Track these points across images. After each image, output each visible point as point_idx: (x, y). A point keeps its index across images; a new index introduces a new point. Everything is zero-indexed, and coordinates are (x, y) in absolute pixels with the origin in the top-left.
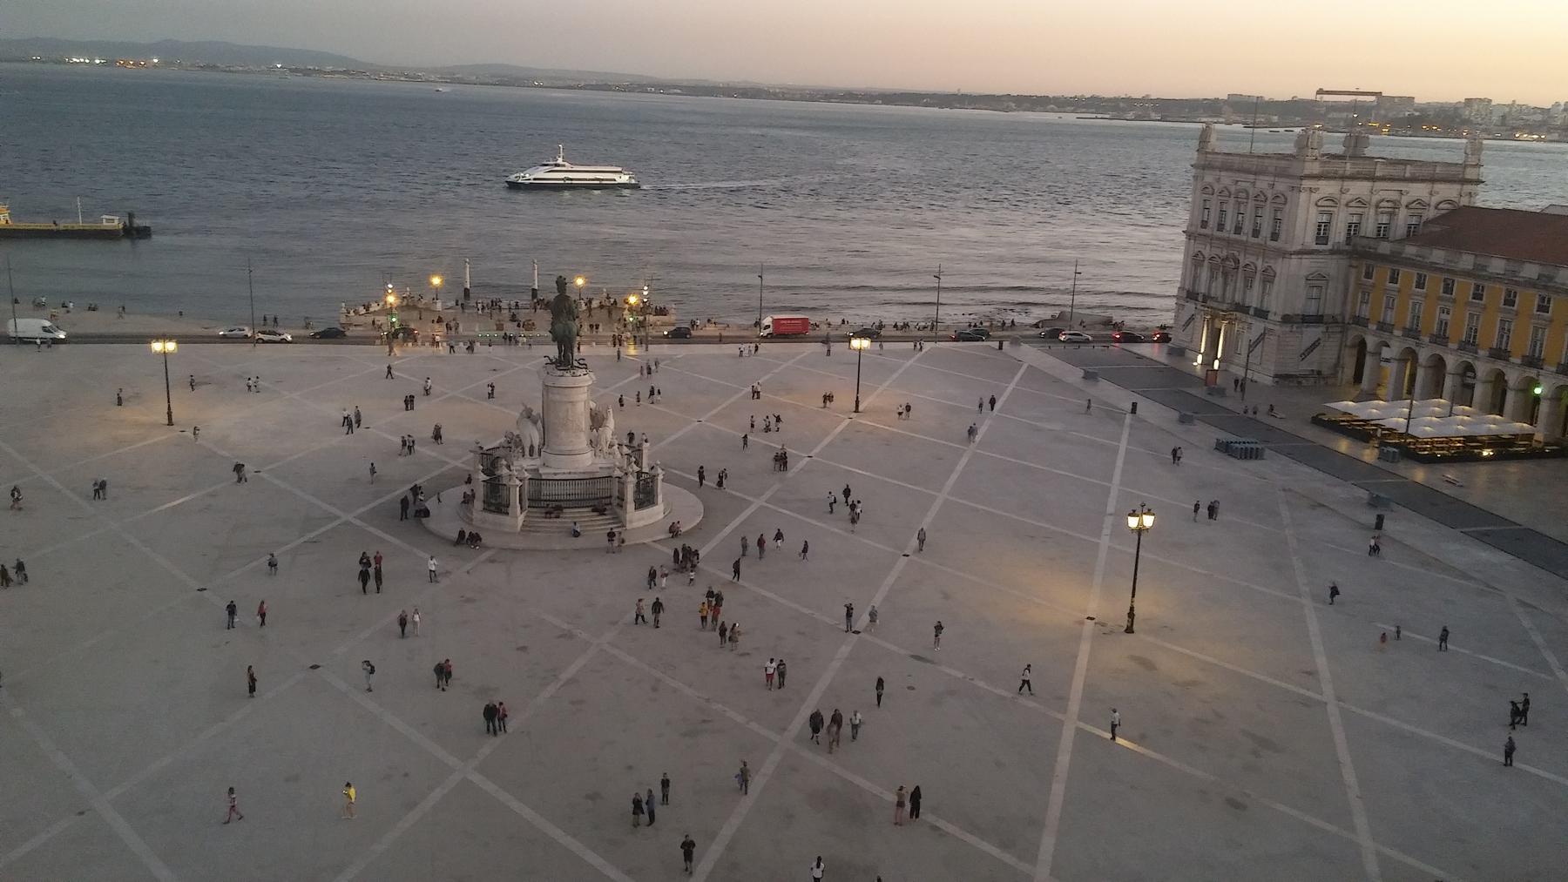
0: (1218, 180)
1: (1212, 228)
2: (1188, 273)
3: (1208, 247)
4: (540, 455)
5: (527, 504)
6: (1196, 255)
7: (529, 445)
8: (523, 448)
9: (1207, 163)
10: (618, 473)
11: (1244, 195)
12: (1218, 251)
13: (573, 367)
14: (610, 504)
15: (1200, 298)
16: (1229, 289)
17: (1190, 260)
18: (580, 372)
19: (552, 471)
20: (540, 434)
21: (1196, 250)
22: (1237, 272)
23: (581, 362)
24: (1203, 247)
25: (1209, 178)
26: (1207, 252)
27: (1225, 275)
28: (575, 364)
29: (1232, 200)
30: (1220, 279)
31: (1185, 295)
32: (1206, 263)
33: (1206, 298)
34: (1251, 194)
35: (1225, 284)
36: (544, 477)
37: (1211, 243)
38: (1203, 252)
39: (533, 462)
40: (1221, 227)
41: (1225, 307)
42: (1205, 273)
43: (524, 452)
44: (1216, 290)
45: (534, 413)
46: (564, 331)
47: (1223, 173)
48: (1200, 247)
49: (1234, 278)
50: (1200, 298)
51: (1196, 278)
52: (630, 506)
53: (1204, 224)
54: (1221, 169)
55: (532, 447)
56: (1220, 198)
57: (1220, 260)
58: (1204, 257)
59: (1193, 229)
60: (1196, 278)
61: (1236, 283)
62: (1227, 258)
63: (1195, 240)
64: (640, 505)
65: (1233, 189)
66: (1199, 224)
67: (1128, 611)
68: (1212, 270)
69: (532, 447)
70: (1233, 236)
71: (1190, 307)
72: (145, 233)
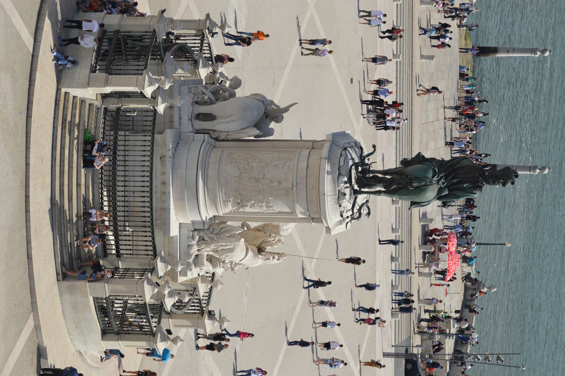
4: (198, 132)
5: (113, 106)
7: (215, 113)
8: (212, 103)
10: (161, 269)
13: (356, 192)
18: (347, 204)
23: (364, 211)
28: (361, 199)
36: (157, 137)
39: (185, 119)
43: (205, 103)
45: (273, 125)
46: (418, 179)
55: (209, 117)
69: (209, 117)
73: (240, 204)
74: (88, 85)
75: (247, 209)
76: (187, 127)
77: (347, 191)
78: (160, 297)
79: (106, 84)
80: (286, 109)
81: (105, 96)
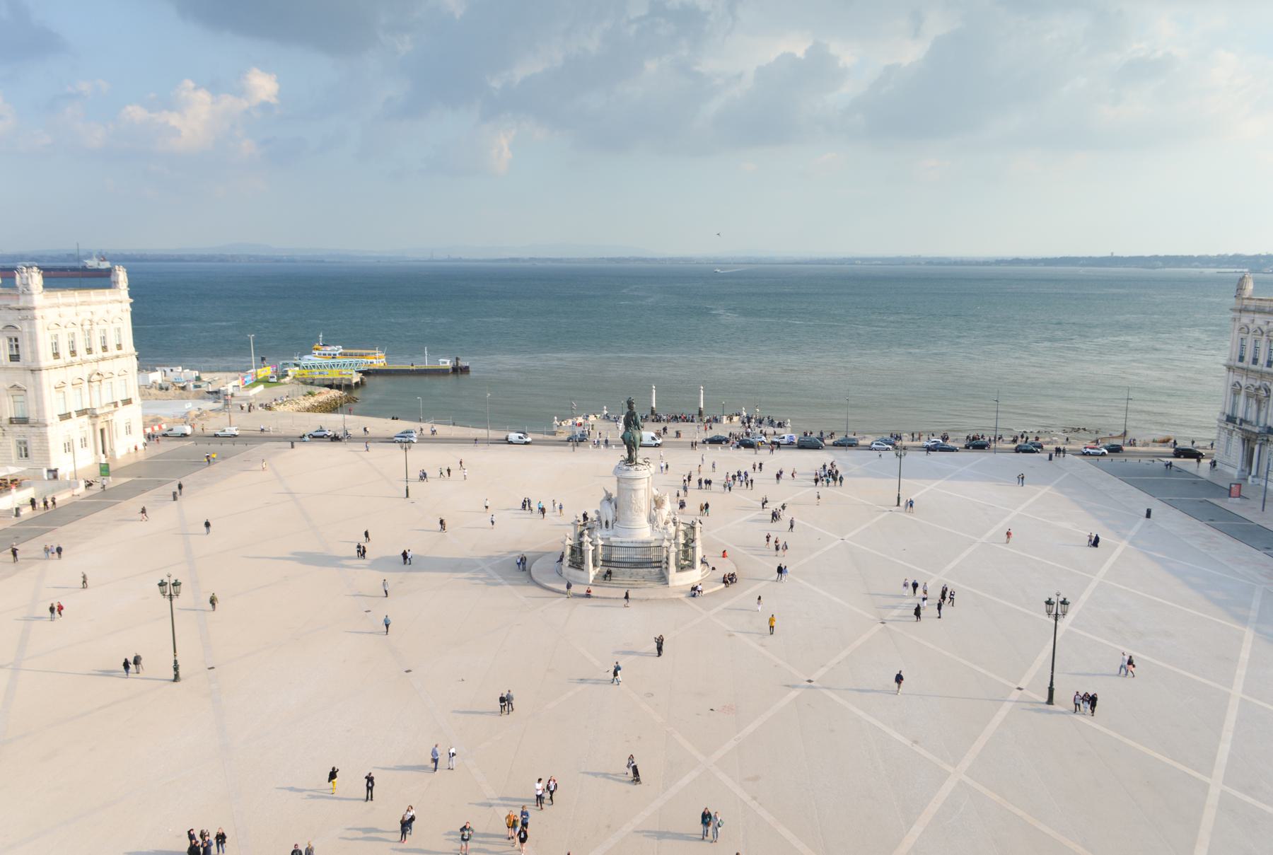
0: (1253, 321)
1: (1248, 363)
2: (1228, 400)
3: (1245, 378)
4: (613, 528)
6: (1235, 385)
8: (601, 522)
9: (1243, 307)
11: (1246, 330)
12: (1252, 382)
14: (661, 567)
15: (1238, 422)
16: (1263, 414)
17: (1230, 388)
19: (619, 539)
20: (613, 512)
21: (1235, 380)
22: (1269, 400)
24: (1240, 378)
25: (1245, 319)
26: (1244, 382)
27: (1259, 402)
29: (1264, 338)
30: (1255, 407)
31: (1224, 418)
32: (1243, 392)
33: (1242, 421)
34: (1251, 329)
35: (1259, 410)
36: (613, 545)
37: (1247, 375)
38: (1241, 382)
39: (608, 533)
40: (1255, 361)
41: (1257, 430)
42: (1242, 400)
43: (601, 525)
44: (1252, 416)
45: (613, 497)
47: (1257, 316)
48: (1237, 378)
49: (1266, 405)
50: (1238, 422)
51: (1234, 405)
52: (672, 568)
53: (1241, 359)
54: (1254, 312)
55: (607, 523)
56: (1254, 336)
57: (1253, 389)
58: (1241, 387)
59: (1232, 363)
60: (1234, 405)
61: (1267, 409)
62: (1258, 389)
63: (1234, 372)
64: (681, 568)
65: (1265, 328)
66: (1237, 358)
67: (1049, 686)
68: (1248, 396)
69: (607, 523)
70: (1265, 369)
71: (1230, 426)
72: (465, 370)
73: (641, 511)
74: (589, 573)
75: (644, 508)
76: (611, 532)
77: (635, 467)
78: (677, 545)
79: (588, 565)
80: (606, 492)
81: (595, 566)
